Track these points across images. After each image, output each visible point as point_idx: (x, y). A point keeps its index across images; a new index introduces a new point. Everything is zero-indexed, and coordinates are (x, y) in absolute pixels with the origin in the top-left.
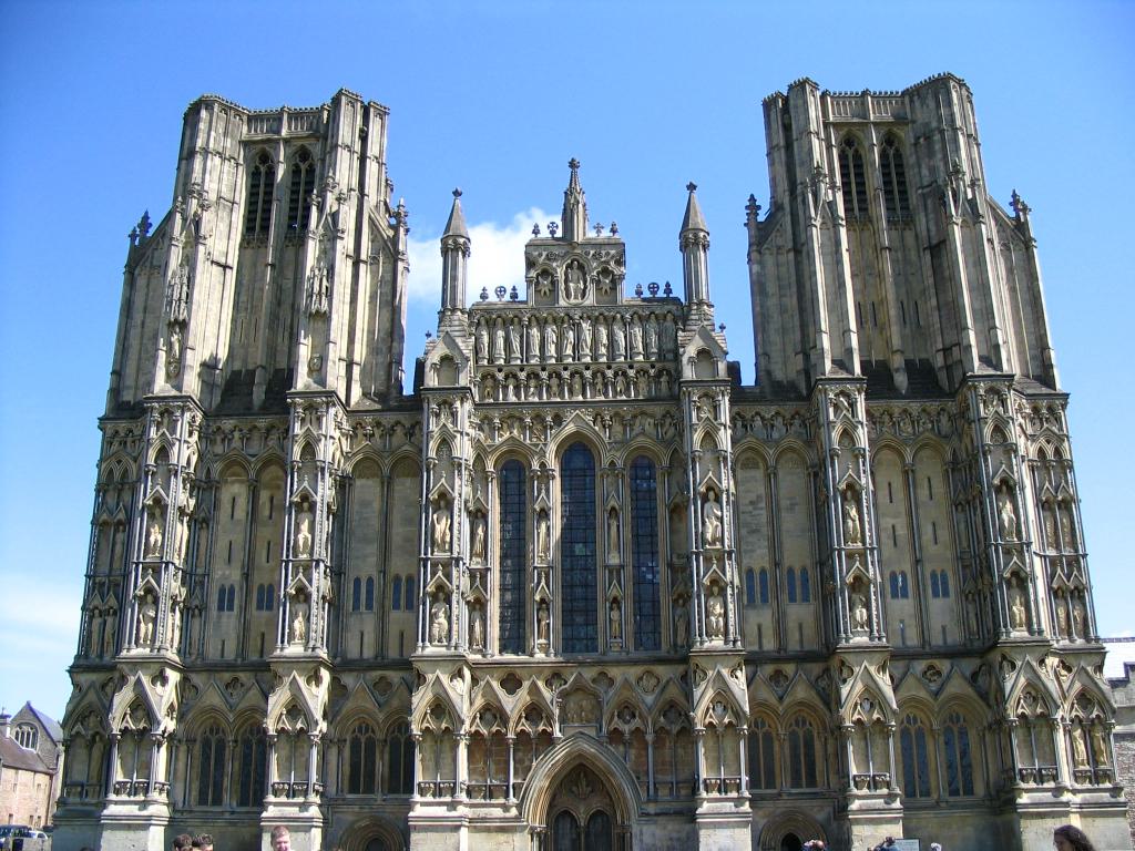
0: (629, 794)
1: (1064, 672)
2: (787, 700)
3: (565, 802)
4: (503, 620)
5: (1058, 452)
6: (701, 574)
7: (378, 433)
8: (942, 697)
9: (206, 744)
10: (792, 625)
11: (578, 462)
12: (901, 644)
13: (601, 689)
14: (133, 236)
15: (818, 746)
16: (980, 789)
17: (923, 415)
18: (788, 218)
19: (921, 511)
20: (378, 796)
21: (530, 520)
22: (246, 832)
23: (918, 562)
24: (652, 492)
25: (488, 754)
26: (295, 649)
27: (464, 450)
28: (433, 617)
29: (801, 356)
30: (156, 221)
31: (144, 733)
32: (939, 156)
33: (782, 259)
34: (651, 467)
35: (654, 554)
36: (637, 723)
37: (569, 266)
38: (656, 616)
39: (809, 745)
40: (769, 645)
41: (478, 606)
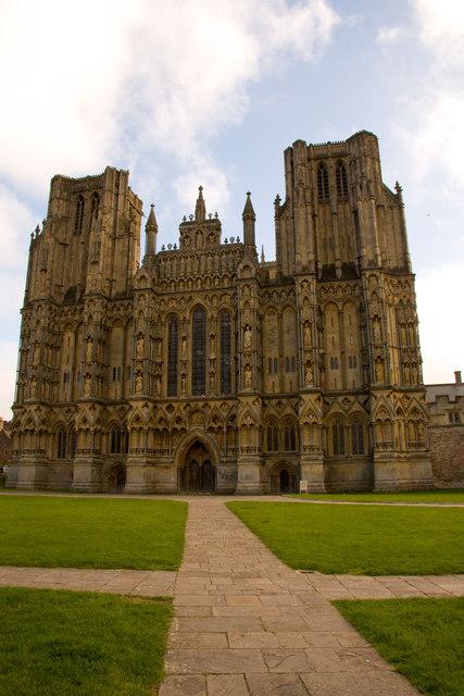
3: (193, 457)
5: (409, 301)
7: (122, 308)
9: (60, 435)
10: (287, 381)
14: (32, 235)
16: (366, 452)
20: (121, 455)
25: (162, 437)
26: (87, 396)
28: (136, 382)
30: (41, 228)
31: (32, 431)
35: (229, 353)
36: (219, 424)
38: (230, 380)
39: (293, 432)
40: (277, 391)
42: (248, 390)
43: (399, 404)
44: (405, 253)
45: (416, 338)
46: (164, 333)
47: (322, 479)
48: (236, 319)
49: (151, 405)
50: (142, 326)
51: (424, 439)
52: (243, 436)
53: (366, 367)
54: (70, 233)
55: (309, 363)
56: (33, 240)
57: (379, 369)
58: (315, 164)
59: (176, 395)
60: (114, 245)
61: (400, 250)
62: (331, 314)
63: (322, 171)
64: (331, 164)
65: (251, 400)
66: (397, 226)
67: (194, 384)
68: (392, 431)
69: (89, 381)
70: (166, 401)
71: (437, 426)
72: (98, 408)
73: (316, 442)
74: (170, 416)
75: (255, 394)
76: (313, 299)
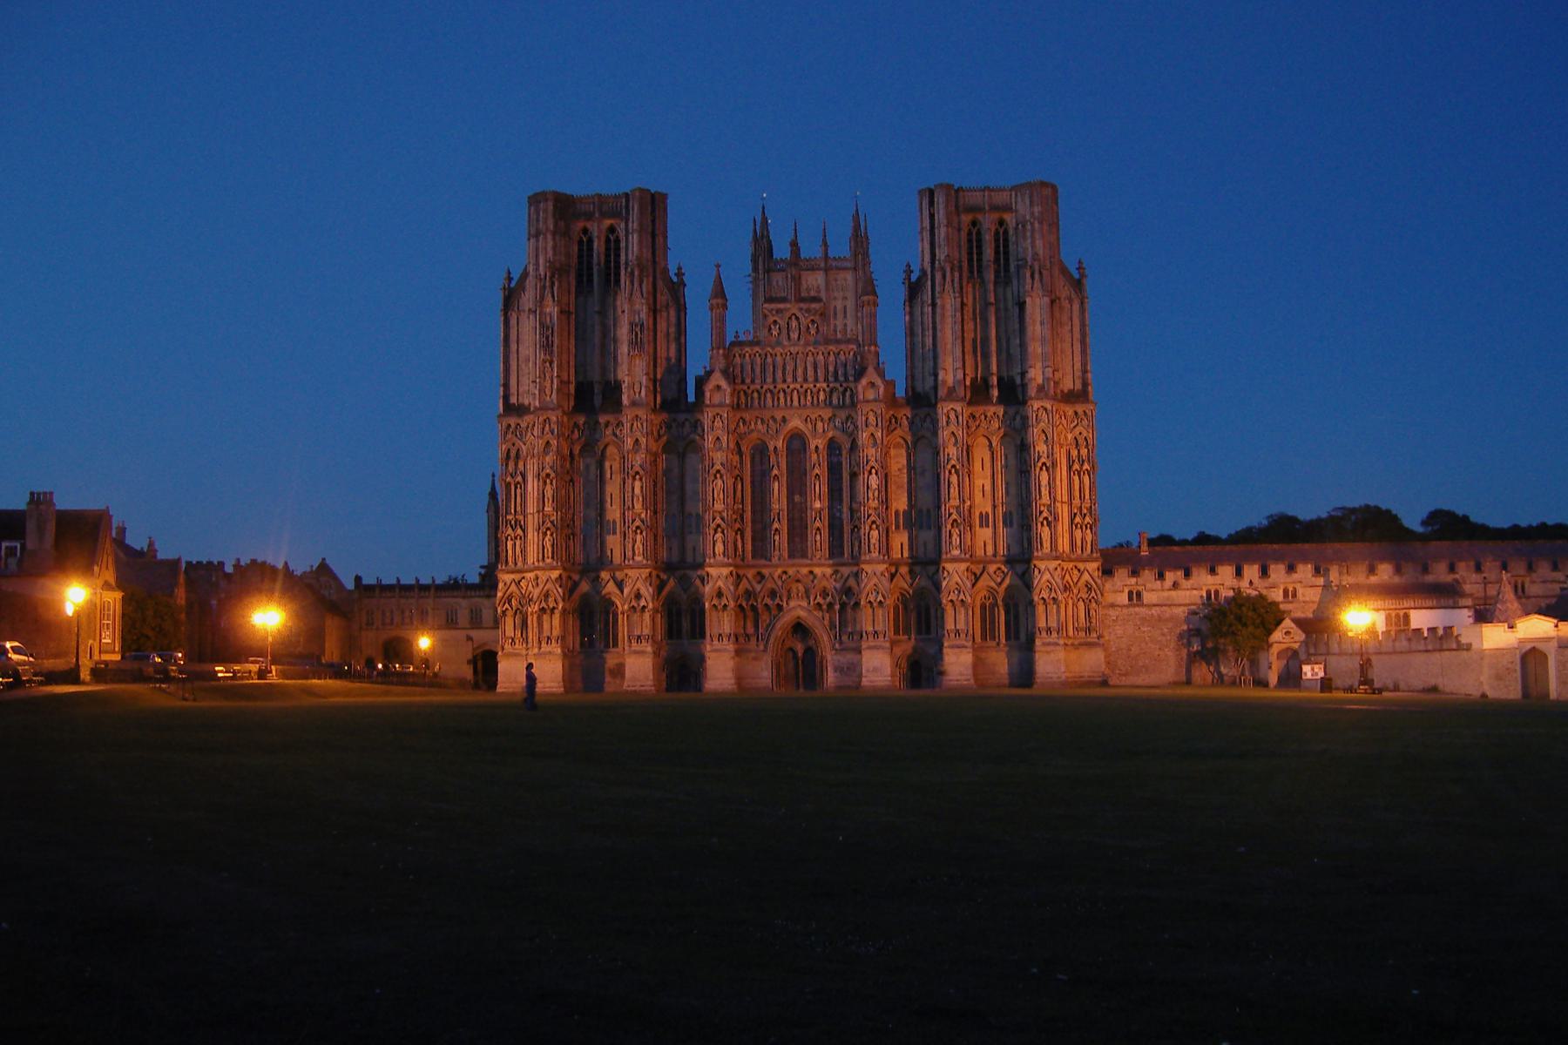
0: (826, 638)
1: (1076, 572)
3: (788, 644)
4: (753, 539)
11: (796, 444)
15: (932, 611)
16: (1023, 637)
18: (929, 283)
29: (933, 378)
30: (516, 276)
32: (1029, 241)
34: (840, 449)
35: (841, 501)
36: (829, 599)
37: (790, 318)
41: (741, 531)
43: (1067, 577)
47: (970, 671)
54: (573, 289)
61: (1078, 366)
68: (1058, 611)
70: (749, 566)
71: (1113, 606)
74: (758, 587)
75: (883, 562)
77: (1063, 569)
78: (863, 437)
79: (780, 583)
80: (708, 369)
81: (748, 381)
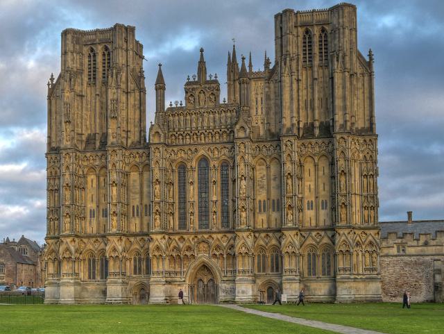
0: (218, 274)
2: (269, 245)
3: (199, 277)
6: (240, 203)
8: (321, 243)
9: (89, 260)
11: (203, 164)
12: (309, 224)
13: (210, 240)
14: (49, 85)
15: (280, 259)
16: (332, 274)
17: (323, 144)
19: (320, 180)
21: (188, 185)
22: (103, 288)
23: (317, 197)
24: (227, 174)
26: (114, 230)
27: (165, 164)
28: (155, 219)
30: (56, 77)
33: (277, 85)
34: (227, 166)
35: (228, 196)
36: (221, 252)
38: (228, 217)
39: (277, 258)
42: (243, 227)
43: (358, 238)
44: (371, 116)
45: (375, 187)
46: (175, 178)
48: (233, 168)
49: (167, 237)
50: (157, 174)
51: (377, 265)
52: (239, 260)
53: (334, 209)
55: (290, 207)
56: (49, 89)
57: (342, 212)
58: (301, 31)
59: (185, 228)
60: (127, 98)
61: (367, 112)
62: (309, 166)
63: (307, 37)
64: (316, 31)
65: (245, 234)
66: (367, 91)
67: (200, 220)
69: (115, 218)
70: (178, 233)
71: (387, 256)
72: (124, 239)
73: (293, 267)
74: (181, 245)
75: (248, 230)
76: (296, 157)
77: (355, 233)
78: (238, 158)
79: (193, 243)
80: (153, 123)
81: (176, 130)
